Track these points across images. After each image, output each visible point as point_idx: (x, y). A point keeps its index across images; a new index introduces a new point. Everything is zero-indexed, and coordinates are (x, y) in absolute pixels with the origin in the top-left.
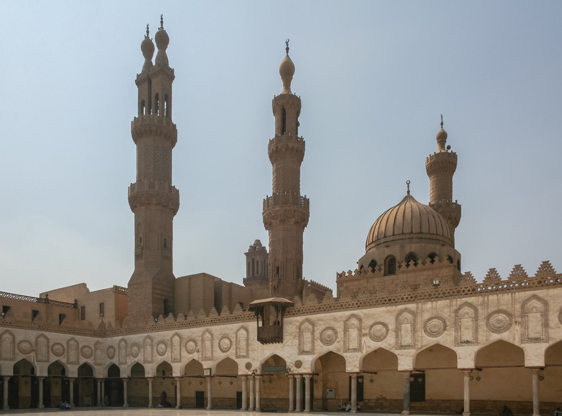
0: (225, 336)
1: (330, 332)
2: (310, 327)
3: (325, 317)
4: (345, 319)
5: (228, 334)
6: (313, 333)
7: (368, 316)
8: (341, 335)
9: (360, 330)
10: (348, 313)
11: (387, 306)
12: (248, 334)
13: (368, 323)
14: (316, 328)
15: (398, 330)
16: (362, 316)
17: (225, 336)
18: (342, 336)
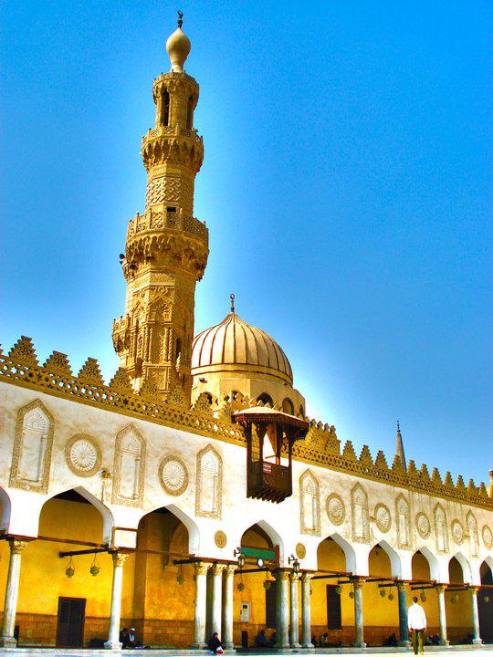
0: (172, 457)
1: (334, 502)
2: (315, 485)
3: (330, 474)
4: (351, 487)
5: (180, 453)
6: (317, 496)
7: (374, 492)
8: (348, 510)
9: (366, 508)
10: (354, 479)
11: (388, 484)
12: (220, 467)
13: (373, 502)
14: (321, 490)
15: (397, 522)
16: (367, 490)
17: (172, 457)
18: (350, 514)
